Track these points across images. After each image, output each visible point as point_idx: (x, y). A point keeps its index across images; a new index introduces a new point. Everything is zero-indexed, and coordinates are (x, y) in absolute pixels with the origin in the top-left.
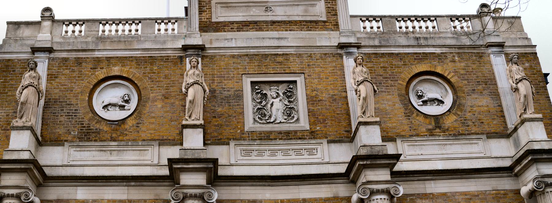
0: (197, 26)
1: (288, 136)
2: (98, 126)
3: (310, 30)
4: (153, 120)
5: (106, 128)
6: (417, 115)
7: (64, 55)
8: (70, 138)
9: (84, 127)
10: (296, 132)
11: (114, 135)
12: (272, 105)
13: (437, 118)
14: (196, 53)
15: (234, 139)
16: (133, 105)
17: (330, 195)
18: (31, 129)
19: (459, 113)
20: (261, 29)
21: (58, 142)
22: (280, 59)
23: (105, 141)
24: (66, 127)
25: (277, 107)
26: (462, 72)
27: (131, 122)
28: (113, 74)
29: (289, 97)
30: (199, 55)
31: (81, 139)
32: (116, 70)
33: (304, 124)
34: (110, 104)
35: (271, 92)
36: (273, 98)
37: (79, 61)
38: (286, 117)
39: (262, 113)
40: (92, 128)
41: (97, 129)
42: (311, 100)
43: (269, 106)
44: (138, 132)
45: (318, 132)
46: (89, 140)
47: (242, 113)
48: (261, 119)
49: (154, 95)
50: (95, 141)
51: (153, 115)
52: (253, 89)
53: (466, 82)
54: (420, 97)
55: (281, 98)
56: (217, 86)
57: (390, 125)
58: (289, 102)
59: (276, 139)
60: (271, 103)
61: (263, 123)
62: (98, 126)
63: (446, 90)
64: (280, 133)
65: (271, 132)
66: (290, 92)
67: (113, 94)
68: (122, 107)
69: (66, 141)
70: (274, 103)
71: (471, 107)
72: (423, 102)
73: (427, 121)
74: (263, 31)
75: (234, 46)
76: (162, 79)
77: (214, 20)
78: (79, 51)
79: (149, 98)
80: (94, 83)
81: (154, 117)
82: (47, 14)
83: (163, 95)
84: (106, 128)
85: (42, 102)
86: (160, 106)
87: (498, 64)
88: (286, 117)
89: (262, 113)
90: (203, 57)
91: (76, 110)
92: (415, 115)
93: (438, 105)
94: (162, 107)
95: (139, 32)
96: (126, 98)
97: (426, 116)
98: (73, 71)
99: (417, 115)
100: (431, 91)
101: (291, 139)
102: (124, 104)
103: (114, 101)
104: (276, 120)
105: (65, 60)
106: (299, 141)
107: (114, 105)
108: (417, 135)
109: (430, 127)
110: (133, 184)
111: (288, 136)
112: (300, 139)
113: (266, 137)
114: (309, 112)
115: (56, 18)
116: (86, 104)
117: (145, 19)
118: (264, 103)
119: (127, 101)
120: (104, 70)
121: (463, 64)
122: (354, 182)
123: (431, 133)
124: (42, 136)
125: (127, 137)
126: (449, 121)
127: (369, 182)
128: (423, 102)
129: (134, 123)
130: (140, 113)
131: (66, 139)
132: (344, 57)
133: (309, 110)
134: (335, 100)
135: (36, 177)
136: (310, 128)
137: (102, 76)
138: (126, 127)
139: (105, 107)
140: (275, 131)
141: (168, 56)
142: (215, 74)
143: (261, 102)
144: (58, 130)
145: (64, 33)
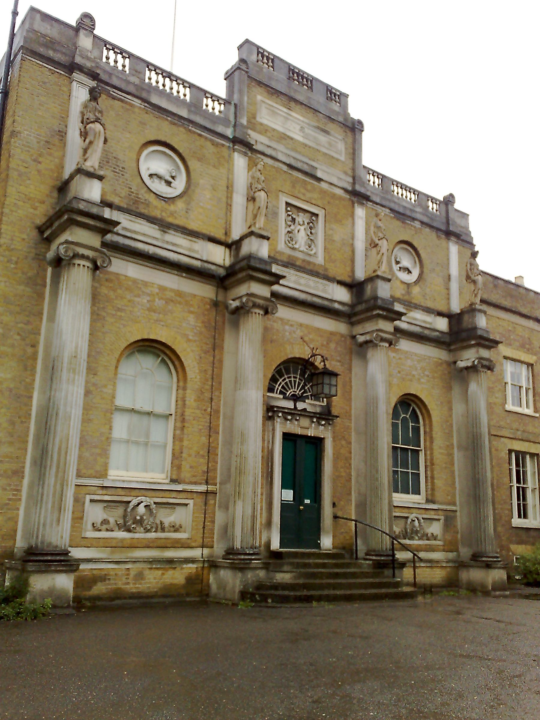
9: (132, 192)
13: (408, 285)
16: (180, 185)
24: (112, 185)
27: (180, 205)
29: (311, 228)
34: (156, 175)
35: (301, 218)
36: (299, 225)
38: (307, 247)
41: (146, 200)
54: (398, 263)
58: (311, 233)
63: (415, 262)
67: (155, 164)
68: (169, 183)
86: (208, 197)
91: (123, 168)
93: (408, 273)
96: (174, 174)
102: (170, 179)
109: (403, 292)
115: (95, 32)
118: (292, 227)
122: (352, 324)
126: (416, 290)
132: (356, 205)
139: (151, 175)
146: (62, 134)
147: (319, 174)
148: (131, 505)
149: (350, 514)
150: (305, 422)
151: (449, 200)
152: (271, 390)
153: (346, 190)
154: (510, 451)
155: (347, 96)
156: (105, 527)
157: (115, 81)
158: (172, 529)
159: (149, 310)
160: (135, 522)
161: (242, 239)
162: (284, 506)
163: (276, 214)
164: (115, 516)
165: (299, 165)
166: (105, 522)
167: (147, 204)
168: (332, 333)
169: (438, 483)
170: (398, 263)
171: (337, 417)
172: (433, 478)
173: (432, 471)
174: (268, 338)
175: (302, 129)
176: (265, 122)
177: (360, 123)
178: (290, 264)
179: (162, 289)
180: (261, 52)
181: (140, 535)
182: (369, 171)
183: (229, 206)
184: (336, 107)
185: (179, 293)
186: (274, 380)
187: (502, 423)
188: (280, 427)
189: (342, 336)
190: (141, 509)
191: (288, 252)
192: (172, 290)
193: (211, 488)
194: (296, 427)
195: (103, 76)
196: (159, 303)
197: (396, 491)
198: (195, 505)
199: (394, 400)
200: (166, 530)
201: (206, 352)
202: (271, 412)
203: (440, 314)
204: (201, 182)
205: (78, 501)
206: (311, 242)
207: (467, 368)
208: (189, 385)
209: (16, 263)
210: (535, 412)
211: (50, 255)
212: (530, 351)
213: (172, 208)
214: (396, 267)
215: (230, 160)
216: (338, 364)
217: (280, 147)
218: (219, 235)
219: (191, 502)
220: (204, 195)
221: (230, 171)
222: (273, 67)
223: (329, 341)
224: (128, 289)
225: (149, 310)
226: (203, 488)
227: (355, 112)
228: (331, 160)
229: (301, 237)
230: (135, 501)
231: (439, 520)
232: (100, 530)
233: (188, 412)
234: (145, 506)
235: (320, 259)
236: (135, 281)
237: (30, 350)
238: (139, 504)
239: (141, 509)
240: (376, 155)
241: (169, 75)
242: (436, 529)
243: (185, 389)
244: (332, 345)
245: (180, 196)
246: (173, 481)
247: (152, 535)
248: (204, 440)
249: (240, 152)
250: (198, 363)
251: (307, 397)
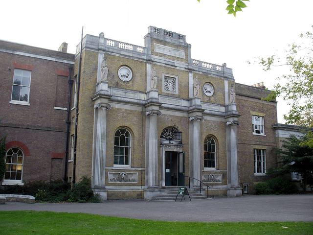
16: (130, 77)
17: (182, 116)
27: (131, 83)
33: (177, 93)
42: (180, 85)
52: (165, 79)
54: (206, 90)
67: (123, 71)
68: (127, 77)
82: (102, 35)
87: (226, 83)
89: (167, 86)
100: (209, 88)
103: (125, 74)
122: (189, 113)
126: (212, 99)
127: (197, 116)
130: (134, 80)
139: (122, 76)
146: (96, 69)
147: (176, 65)
149: (189, 175)
150: (173, 147)
151: (224, 65)
152: (161, 137)
153: (186, 68)
154: (254, 149)
155: (185, 36)
157: (110, 50)
159: (122, 117)
160: (122, 179)
161: (150, 91)
162: (166, 173)
163: (161, 80)
165: (169, 63)
166: (114, 179)
168: (182, 117)
169: (221, 163)
170: (206, 90)
172: (219, 162)
173: (218, 159)
174: (159, 121)
175: (170, 51)
177: (190, 45)
178: (167, 95)
179: (126, 110)
180: (155, 29)
182: (194, 60)
183: (146, 80)
184: (181, 41)
185: (131, 111)
186: (162, 134)
187: (251, 140)
188: (164, 150)
189: (185, 117)
190: (123, 175)
191: (166, 92)
192: (129, 110)
193: (143, 169)
194: (169, 149)
195: (107, 49)
196: (125, 114)
197: (205, 166)
199: (204, 137)
201: (140, 128)
202: (161, 145)
203: (221, 105)
204: (137, 75)
205: (106, 173)
206: (174, 88)
207: (230, 124)
208: (135, 139)
210: (265, 134)
211: (95, 106)
212: (263, 112)
213: (128, 85)
214: (205, 91)
215: (146, 65)
217: (163, 58)
218: (143, 90)
219: (137, 173)
220: (138, 79)
221: (146, 70)
223: (181, 120)
224: (116, 112)
225: (122, 117)
226: (141, 169)
227: (188, 41)
228: (179, 59)
229: (170, 86)
230: (121, 173)
233: (135, 147)
235: (177, 93)
236: (118, 109)
237: (91, 132)
239: (123, 175)
240: (196, 54)
241: (127, 44)
242: (220, 178)
243: (134, 140)
244: (182, 121)
245: (130, 80)
246: (132, 167)
247: (126, 182)
248: (140, 155)
249: (148, 63)
251: (174, 139)
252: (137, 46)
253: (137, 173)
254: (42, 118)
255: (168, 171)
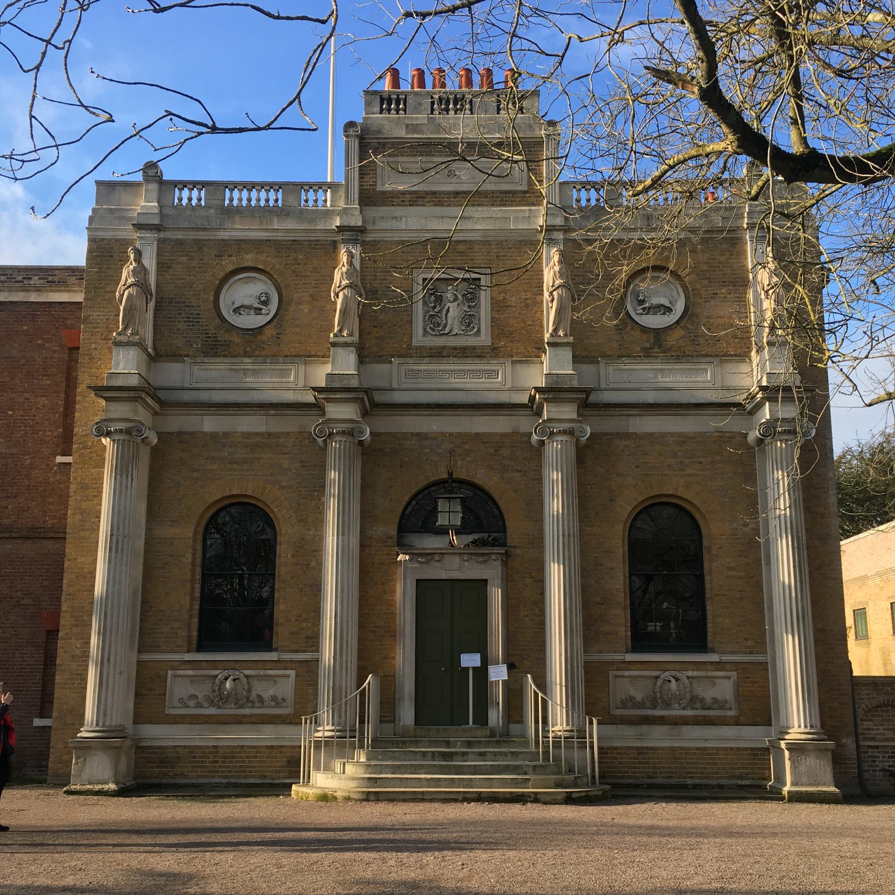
0: (357, 196)
1: (464, 353)
2: (227, 337)
3: (505, 205)
4: (297, 330)
5: (237, 340)
6: (633, 328)
7: (179, 235)
8: (191, 353)
9: (210, 337)
10: (474, 348)
11: (248, 349)
12: (448, 311)
13: (658, 333)
14: (354, 237)
15: (398, 356)
18: (141, 345)
19: (689, 326)
20: (439, 204)
21: (175, 356)
22: (461, 248)
23: (236, 356)
24: (186, 337)
25: (454, 311)
26: (704, 267)
27: (269, 332)
28: (245, 265)
30: (358, 240)
31: (206, 354)
32: (249, 259)
34: (242, 306)
37: (199, 244)
39: (434, 322)
40: (219, 338)
41: (225, 341)
43: (444, 312)
44: (279, 345)
45: (502, 349)
46: (216, 355)
47: (411, 322)
48: (434, 330)
49: (299, 295)
50: (225, 356)
51: (297, 322)
53: (705, 282)
55: (459, 301)
56: (380, 284)
57: (594, 342)
58: (469, 307)
59: (449, 356)
60: (446, 308)
61: (436, 335)
62: (227, 337)
64: (455, 348)
65: (444, 348)
66: (471, 293)
67: (245, 291)
68: (258, 311)
69: (187, 356)
70: (451, 309)
71: (708, 317)
72: (644, 309)
73: (645, 337)
74: (442, 205)
75: (403, 227)
76: (309, 273)
77: (379, 188)
78: (197, 229)
79: (292, 300)
80: (220, 277)
81: (298, 326)
83: (311, 296)
84: (237, 340)
85: (152, 305)
86: (306, 310)
88: (463, 328)
89: (434, 322)
90: (364, 244)
92: (629, 328)
93: (664, 314)
94: (310, 312)
95: (280, 203)
96: (262, 299)
97: (645, 330)
98: (192, 259)
99: (633, 328)
101: (467, 357)
103: (247, 302)
104: (451, 331)
105: (181, 242)
106: (477, 361)
107: (249, 307)
108: (628, 356)
109: (647, 345)
110: (272, 412)
111: (464, 353)
112: (479, 356)
113: (438, 354)
114: (492, 322)
116: (211, 305)
117: (287, 184)
119: (265, 303)
120: (234, 259)
121: (707, 255)
123: (647, 354)
124: (154, 349)
125: (264, 353)
128: (644, 309)
129: (275, 333)
131: (186, 353)
133: (492, 318)
134: (527, 306)
135: (149, 406)
136: (493, 344)
137: (231, 268)
138: (264, 338)
139: (237, 310)
140: (448, 347)
141: (317, 241)
142: (377, 268)
143: (435, 307)
144: (176, 341)
145: (176, 201)
148: (217, 681)
156: (192, 703)
158: (273, 704)
164: (203, 691)
167: (228, 344)
171: (515, 547)
176: (388, 187)
181: (230, 710)
192: (257, 434)
198: (297, 676)
200: (266, 704)
209: (91, 447)
216: (517, 474)
219: (292, 673)
222: (405, 110)
231: (729, 678)
232: (188, 707)
234: (234, 680)
235: (485, 339)
236: (213, 436)
238: (226, 679)
241: (262, 186)
244: (505, 452)
250: (295, 512)
252: (301, 185)
253: (292, 673)
254: (15, 497)
255: (471, 660)
